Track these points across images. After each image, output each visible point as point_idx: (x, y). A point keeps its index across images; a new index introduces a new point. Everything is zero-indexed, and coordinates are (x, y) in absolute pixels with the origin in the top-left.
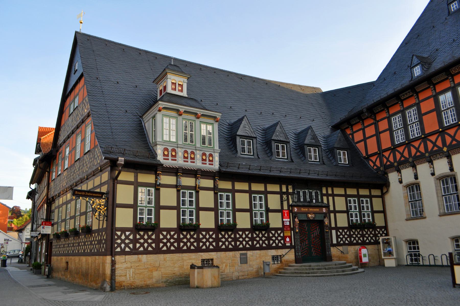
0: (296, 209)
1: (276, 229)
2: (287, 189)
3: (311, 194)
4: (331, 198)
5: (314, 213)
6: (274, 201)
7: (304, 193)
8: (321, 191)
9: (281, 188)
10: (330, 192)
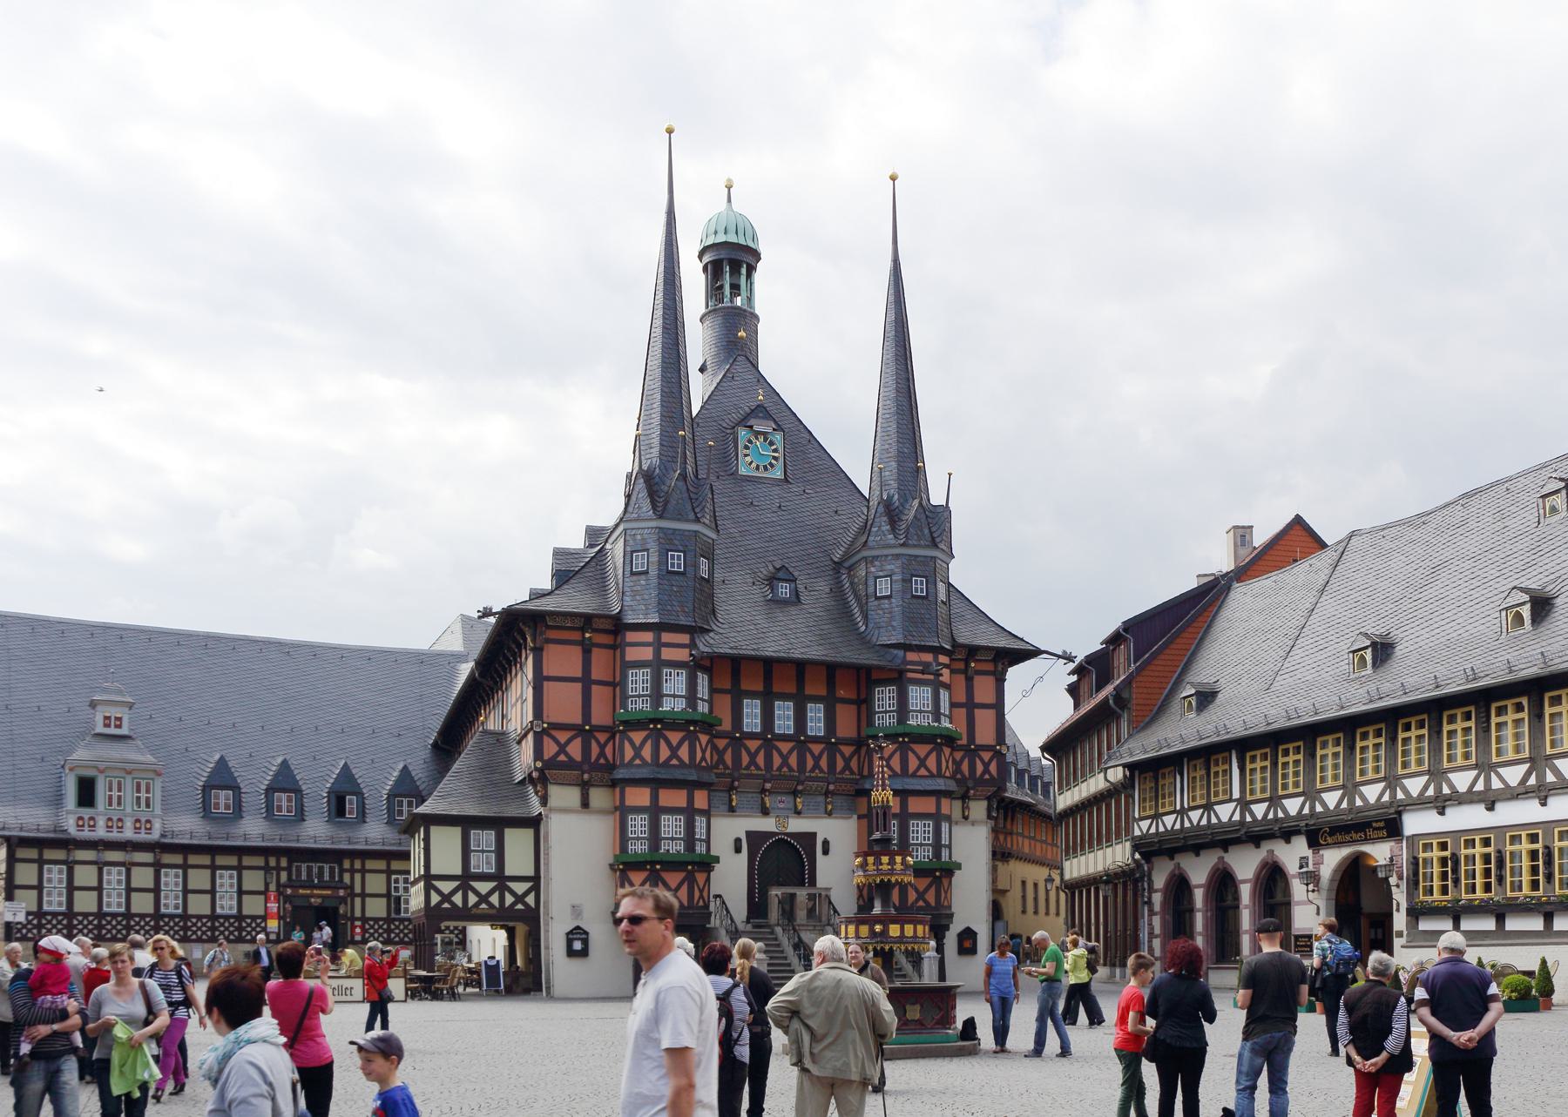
0: (289, 891)
1: (254, 918)
2: (278, 862)
3: (321, 869)
4: (358, 877)
5: (319, 896)
6: (253, 880)
7: (309, 869)
8: (341, 865)
9: (267, 862)
10: (358, 865)
